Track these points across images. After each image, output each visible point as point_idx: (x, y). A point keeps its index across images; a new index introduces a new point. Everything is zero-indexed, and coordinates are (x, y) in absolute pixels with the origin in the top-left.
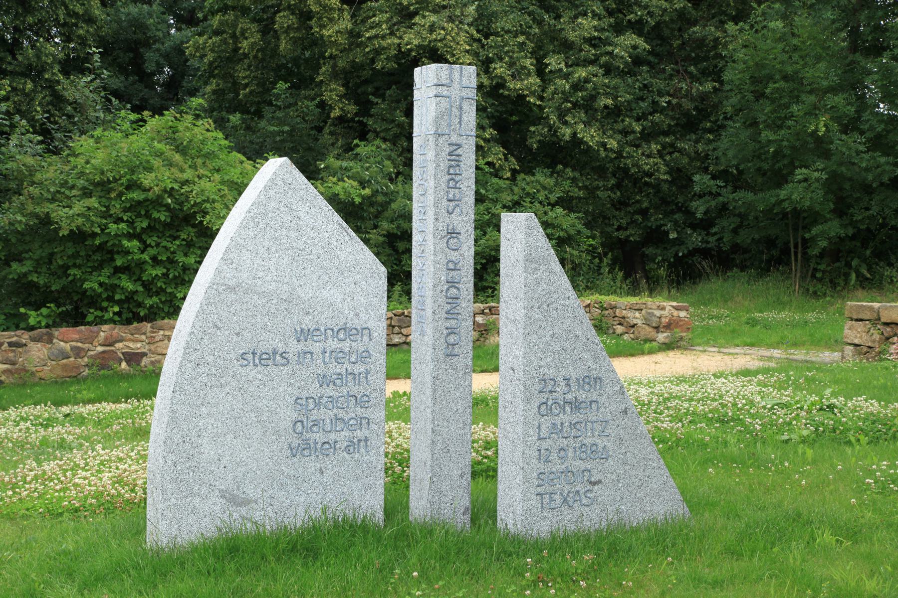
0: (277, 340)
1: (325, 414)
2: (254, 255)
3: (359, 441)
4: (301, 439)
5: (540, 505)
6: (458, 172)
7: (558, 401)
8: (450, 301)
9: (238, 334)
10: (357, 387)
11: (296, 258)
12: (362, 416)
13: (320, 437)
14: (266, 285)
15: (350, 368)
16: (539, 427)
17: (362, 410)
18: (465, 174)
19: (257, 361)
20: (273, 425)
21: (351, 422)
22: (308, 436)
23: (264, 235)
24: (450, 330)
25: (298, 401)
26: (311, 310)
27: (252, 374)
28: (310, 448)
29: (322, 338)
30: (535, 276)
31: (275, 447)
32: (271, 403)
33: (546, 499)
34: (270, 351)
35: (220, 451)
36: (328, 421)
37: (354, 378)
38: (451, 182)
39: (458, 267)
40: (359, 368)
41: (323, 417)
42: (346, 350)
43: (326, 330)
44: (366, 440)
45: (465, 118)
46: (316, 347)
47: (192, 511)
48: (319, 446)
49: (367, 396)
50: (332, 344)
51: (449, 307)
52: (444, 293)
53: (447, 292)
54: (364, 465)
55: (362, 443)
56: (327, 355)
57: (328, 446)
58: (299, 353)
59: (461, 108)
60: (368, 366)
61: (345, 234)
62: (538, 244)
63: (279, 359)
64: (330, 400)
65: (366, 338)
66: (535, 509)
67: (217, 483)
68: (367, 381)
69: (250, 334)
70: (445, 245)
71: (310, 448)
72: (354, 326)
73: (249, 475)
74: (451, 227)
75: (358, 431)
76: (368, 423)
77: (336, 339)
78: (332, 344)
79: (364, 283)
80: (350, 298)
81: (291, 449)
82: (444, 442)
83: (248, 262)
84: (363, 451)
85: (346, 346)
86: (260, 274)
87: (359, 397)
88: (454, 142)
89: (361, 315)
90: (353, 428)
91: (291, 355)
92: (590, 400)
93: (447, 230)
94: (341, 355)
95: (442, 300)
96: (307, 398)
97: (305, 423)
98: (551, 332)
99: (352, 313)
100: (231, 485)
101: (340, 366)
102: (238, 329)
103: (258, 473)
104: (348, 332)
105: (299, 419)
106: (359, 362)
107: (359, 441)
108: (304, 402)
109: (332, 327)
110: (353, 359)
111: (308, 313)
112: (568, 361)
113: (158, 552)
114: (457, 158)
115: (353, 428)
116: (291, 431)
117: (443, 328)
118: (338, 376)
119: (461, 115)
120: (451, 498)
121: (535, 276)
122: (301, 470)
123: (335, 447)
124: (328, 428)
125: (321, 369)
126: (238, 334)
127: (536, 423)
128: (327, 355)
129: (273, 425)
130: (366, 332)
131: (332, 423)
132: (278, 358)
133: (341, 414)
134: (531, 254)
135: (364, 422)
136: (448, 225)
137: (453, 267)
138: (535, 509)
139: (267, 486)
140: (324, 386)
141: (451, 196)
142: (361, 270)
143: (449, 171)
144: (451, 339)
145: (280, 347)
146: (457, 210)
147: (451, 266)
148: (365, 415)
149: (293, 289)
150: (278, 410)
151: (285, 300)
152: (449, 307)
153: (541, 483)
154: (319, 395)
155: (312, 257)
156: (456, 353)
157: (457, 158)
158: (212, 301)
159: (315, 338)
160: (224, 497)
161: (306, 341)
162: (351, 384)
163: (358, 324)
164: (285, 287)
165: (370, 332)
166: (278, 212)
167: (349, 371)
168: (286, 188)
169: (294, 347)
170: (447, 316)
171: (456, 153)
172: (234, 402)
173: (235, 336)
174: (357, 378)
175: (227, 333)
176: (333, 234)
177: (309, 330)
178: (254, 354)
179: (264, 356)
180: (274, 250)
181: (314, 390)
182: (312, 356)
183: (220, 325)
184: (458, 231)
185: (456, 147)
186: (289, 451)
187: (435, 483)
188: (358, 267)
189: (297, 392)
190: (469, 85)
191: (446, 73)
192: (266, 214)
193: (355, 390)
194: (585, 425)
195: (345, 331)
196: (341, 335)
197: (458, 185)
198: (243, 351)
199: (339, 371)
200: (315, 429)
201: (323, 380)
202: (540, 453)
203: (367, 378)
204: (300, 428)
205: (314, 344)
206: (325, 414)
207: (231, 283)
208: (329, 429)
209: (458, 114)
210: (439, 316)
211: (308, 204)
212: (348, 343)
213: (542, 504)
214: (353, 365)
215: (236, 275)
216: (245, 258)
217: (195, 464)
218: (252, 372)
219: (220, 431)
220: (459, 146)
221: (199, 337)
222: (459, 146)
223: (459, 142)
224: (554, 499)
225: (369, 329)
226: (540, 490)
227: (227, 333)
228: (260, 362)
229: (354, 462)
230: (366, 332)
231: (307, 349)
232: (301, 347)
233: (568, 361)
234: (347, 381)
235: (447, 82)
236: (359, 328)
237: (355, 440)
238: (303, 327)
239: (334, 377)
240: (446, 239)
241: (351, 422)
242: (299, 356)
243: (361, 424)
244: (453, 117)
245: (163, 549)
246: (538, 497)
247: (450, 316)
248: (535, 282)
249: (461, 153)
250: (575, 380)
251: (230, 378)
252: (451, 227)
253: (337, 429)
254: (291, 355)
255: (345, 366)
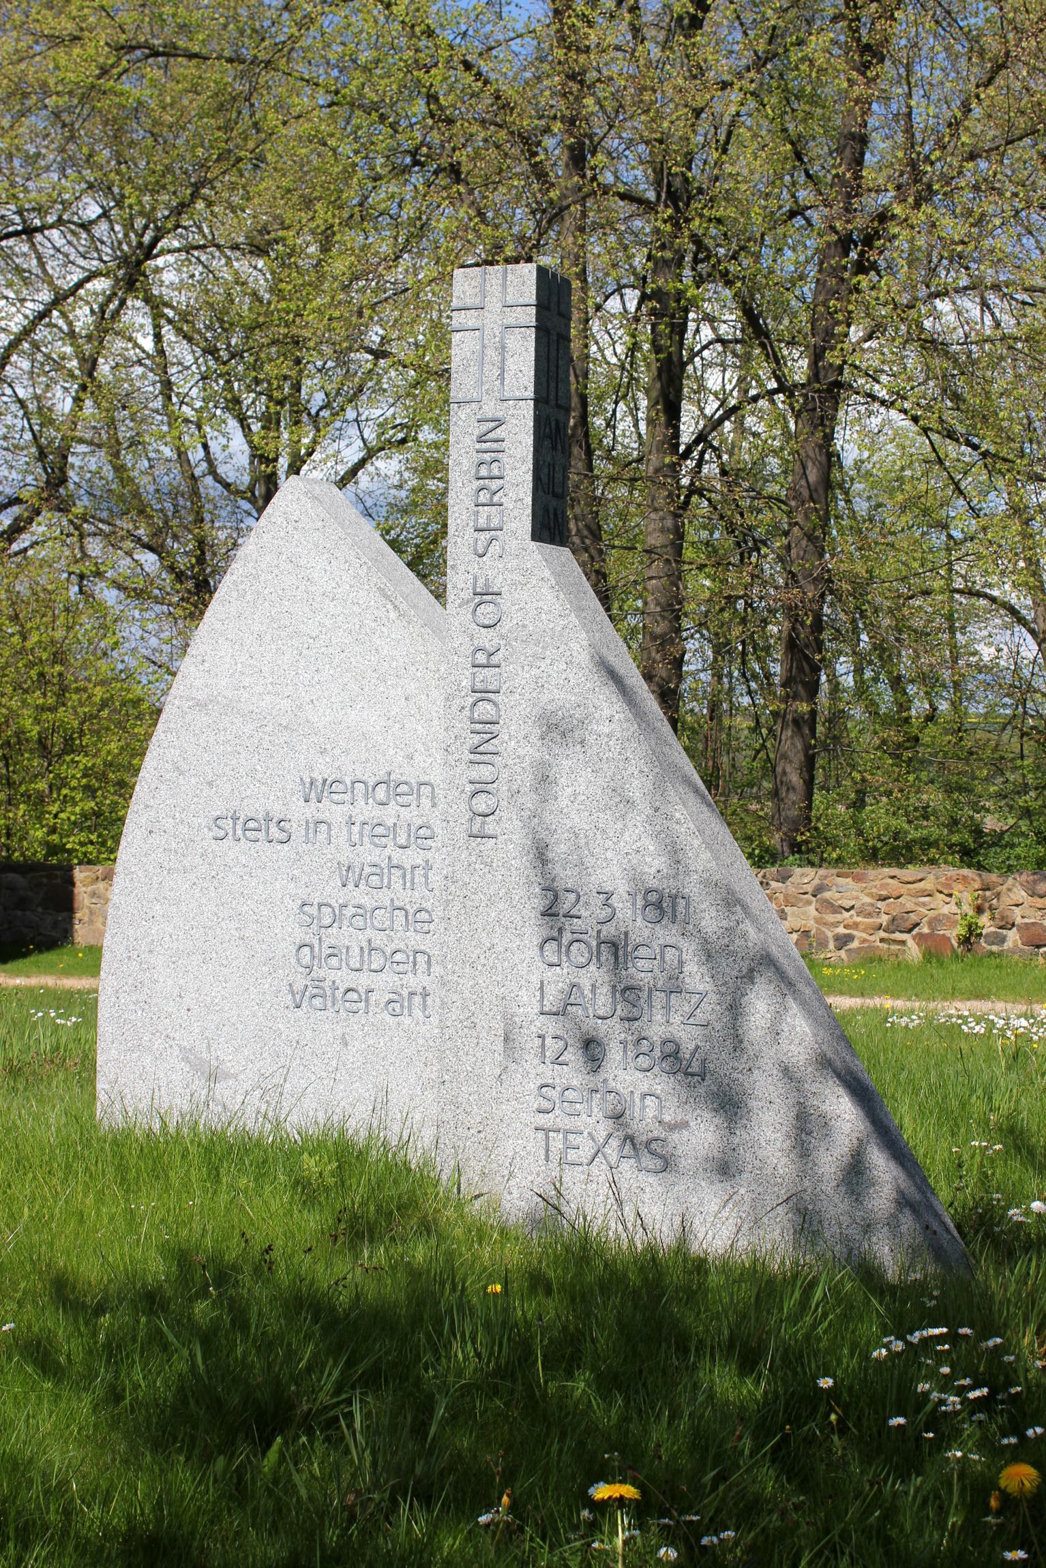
0: (272, 798)
1: (346, 936)
2: (236, 647)
3: (412, 994)
4: (309, 978)
5: (543, 1152)
6: (496, 472)
7: (584, 937)
8: (479, 727)
9: (210, 784)
10: (410, 892)
11: (305, 652)
12: (417, 948)
13: (344, 978)
14: (254, 700)
15: (398, 856)
16: (542, 988)
17: (418, 938)
18: (510, 475)
19: (239, 832)
20: (264, 947)
21: (398, 957)
22: (322, 973)
23: (254, 613)
24: (478, 786)
25: (306, 908)
26: (328, 746)
27: (231, 855)
28: (324, 996)
29: (347, 797)
30: (534, 672)
31: (267, 986)
32: (261, 907)
33: (557, 1142)
34: (260, 816)
35: (181, 981)
36: (357, 950)
37: (404, 876)
38: (481, 493)
39: (495, 660)
40: (413, 857)
41: (347, 943)
42: (390, 822)
43: (353, 783)
44: (425, 995)
45: (511, 364)
46: (335, 813)
47: (141, 1075)
48: (339, 994)
49: (427, 911)
50: (366, 811)
51: (477, 739)
52: (467, 712)
53: (472, 710)
54: (421, 1042)
55: (417, 1000)
56: (356, 829)
57: (354, 996)
58: (307, 822)
59: (503, 347)
60: (429, 855)
61: (390, 606)
62: (540, 604)
63: (275, 832)
64: (360, 911)
65: (426, 802)
66: (531, 1159)
67: (177, 1035)
68: (427, 883)
69: (228, 786)
70: (470, 616)
71: (324, 996)
72: (404, 779)
73: (225, 1029)
74: (481, 582)
75: (410, 975)
76: (429, 963)
77: (371, 801)
78: (366, 811)
79: (424, 697)
80: (397, 726)
81: (293, 995)
82: (464, 1007)
83: (228, 659)
84: (418, 1013)
85: (389, 815)
86: (247, 681)
87: (411, 911)
88: (490, 415)
89: (418, 758)
90: (401, 968)
91: (295, 826)
92: (661, 942)
93: (475, 587)
94: (380, 830)
95: (462, 725)
96: (320, 905)
97: (316, 949)
98: (569, 790)
99: (402, 753)
100: (198, 1043)
101: (378, 851)
102: (211, 774)
103: (241, 1027)
104: (393, 786)
105: (307, 941)
106: (413, 847)
107: (412, 994)
108: (313, 910)
109: (365, 778)
110: (402, 840)
111: (323, 752)
112: (609, 854)
113: (120, 1141)
114: (495, 446)
115: (401, 968)
116: (293, 961)
117: (464, 780)
118: (374, 869)
119: (503, 361)
120: (478, 1119)
121: (534, 672)
122: (309, 1034)
123: (367, 1001)
124: (355, 963)
125: (346, 855)
126: (210, 784)
127: (535, 979)
128: (356, 829)
129: (264, 947)
130: (425, 790)
131: (362, 956)
132: (274, 830)
133: (379, 939)
134: (524, 626)
135: (421, 959)
136: (475, 579)
137: (485, 661)
138: (531, 1159)
139: (254, 1053)
140: (351, 886)
141: (482, 522)
142: (419, 674)
143: (478, 471)
144: (481, 804)
145: (277, 811)
146: (495, 548)
147: (481, 658)
148: (423, 948)
149: (300, 707)
150: (273, 920)
151: (286, 727)
152: (477, 739)
153: (546, 1105)
154: (341, 901)
155: (330, 650)
156: (491, 832)
157: (495, 446)
158: (172, 725)
159: (335, 797)
160: (186, 1060)
161: (320, 802)
162: (397, 885)
163: (411, 775)
164: (286, 704)
165: (433, 792)
166: (276, 571)
167: (395, 862)
168: (290, 528)
169: (300, 811)
170: (472, 757)
171: (491, 436)
172: (204, 901)
173: (205, 787)
174: (408, 877)
175: (193, 780)
176: (368, 607)
177: (325, 781)
178: (235, 819)
179: (251, 825)
180: (268, 637)
181: (333, 893)
182: (330, 829)
183: (185, 767)
184: (495, 589)
185: (493, 424)
186: (290, 997)
187: (447, 1085)
188: (413, 668)
189: (303, 893)
190: (521, 301)
191: (474, 283)
192: (257, 577)
193: (404, 897)
194: (650, 996)
195: (388, 787)
196: (381, 793)
197: (496, 499)
198: (218, 813)
199: (376, 860)
200: (334, 961)
201: (349, 874)
202: (543, 1045)
203: (426, 878)
204: (308, 958)
205: (334, 807)
206: (346, 936)
207: (200, 696)
208: (358, 966)
209: (497, 359)
210: (456, 756)
211: (326, 555)
212: (393, 808)
213: (547, 1151)
214: (401, 851)
215: (210, 681)
216: (223, 653)
217: (143, 997)
218: (233, 851)
219: (181, 948)
220: (500, 422)
221: (153, 786)
222: (500, 422)
223: (499, 414)
224: (575, 1143)
225: (432, 786)
226: (542, 1120)
227: (193, 780)
228: (244, 835)
229: (402, 1033)
230: (425, 790)
231: (321, 817)
232: (310, 811)
233: (609, 854)
234: (390, 879)
235: (477, 302)
236: (413, 781)
237: (405, 993)
238: (315, 775)
239: (367, 870)
240: (472, 605)
241: (398, 957)
242: (307, 829)
243: (415, 964)
244: (487, 367)
245: (775, 1276)
246: (541, 1134)
247: (478, 758)
248: (533, 686)
249: (503, 435)
250: (625, 896)
251: (198, 860)
252: (481, 582)
253: (373, 967)
254: (295, 826)
255: (387, 852)
